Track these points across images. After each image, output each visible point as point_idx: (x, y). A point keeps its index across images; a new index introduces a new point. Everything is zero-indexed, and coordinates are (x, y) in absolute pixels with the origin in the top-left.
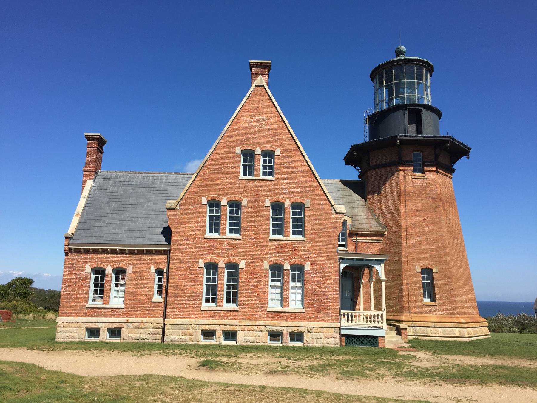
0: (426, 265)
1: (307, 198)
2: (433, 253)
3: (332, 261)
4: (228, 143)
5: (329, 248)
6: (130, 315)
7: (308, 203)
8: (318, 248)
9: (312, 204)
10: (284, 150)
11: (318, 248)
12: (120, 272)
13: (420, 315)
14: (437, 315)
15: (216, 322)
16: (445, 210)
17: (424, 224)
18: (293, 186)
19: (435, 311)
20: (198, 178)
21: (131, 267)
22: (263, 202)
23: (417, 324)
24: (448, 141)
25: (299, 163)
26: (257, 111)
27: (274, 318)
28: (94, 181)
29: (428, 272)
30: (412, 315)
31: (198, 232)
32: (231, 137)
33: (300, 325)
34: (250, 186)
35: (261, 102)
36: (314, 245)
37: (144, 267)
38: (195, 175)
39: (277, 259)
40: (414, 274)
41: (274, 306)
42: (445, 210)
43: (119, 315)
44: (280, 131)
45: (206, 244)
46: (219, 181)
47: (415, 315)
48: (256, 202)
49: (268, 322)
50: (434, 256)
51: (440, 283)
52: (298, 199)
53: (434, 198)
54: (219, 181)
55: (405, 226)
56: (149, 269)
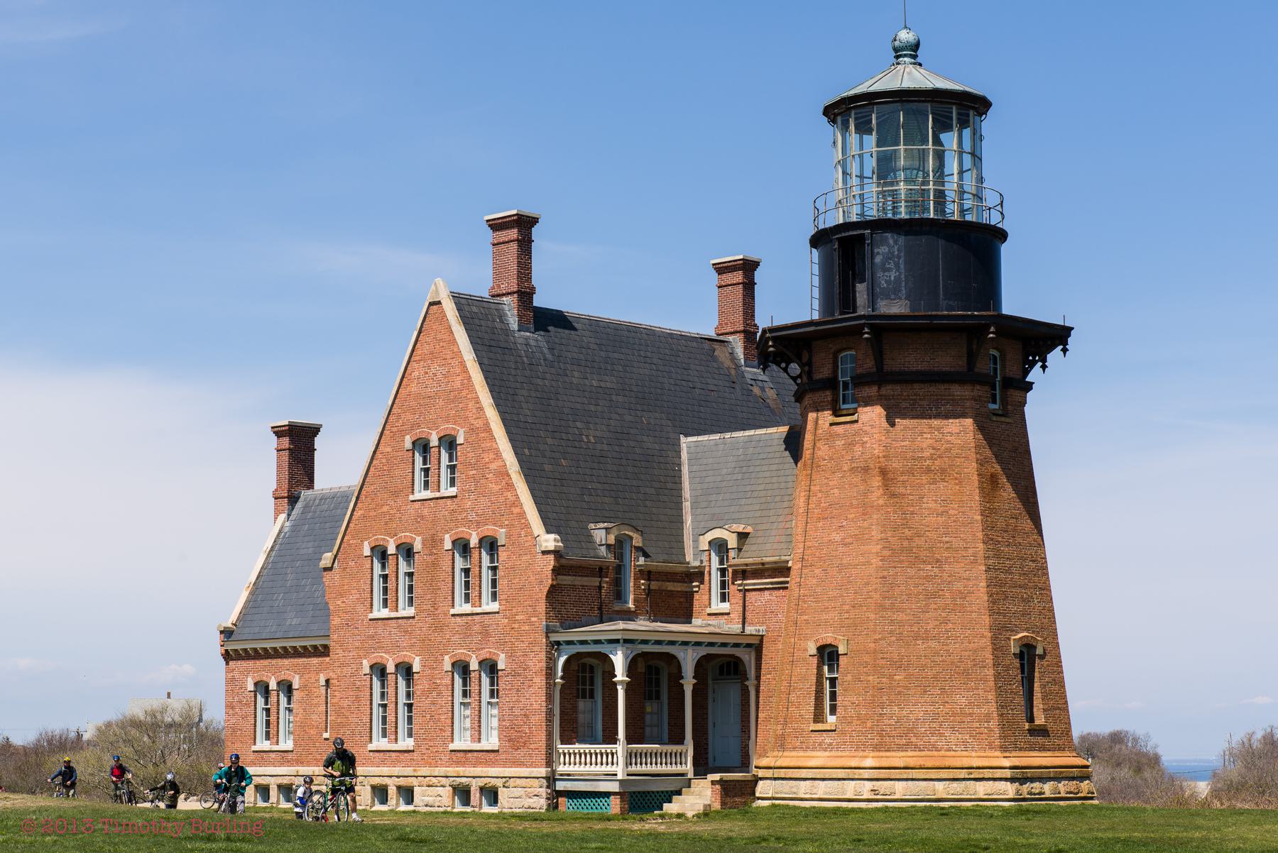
0: (828, 637)
1: (501, 526)
2: (846, 607)
3: (535, 649)
4: (394, 429)
5: (532, 624)
6: (299, 762)
7: (501, 535)
8: (516, 626)
9: (508, 536)
10: (472, 430)
11: (516, 626)
12: (287, 688)
13: (801, 754)
14: (833, 753)
15: (385, 770)
16: (893, 495)
17: (837, 537)
18: (484, 501)
19: (831, 744)
20: (359, 505)
21: (297, 677)
22: (442, 540)
23: (782, 773)
24: (863, 326)
25: (492, 456)
26: (433, 356)
27: (458, 763)
28: (289, 515)
29: (828, 655)
30: (786, 754)
31: (360, 608)
32: (399, 416)
33: (492, 773)
34: (426, 512)
35: (439, 336)
36: (512, 619)
37: (313, 675)
38: (354, 499)
39: (461, 652)
40: (805, 659)
41: (462, 741)
42: (893, 495)
43: (289, 763)
44: (464, 393)
45: (372, 632)
46: (385, 509)
47: (794, 754)
48: (433, 542)
49: (451, 771)
50: (846, 615)
51: (849, 677)
52: (488, 530)
53: (866, 470)
54: (385, 509)
55: (801, 546)
56: (318, 680)
